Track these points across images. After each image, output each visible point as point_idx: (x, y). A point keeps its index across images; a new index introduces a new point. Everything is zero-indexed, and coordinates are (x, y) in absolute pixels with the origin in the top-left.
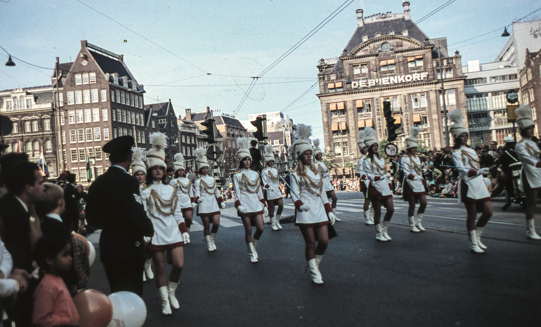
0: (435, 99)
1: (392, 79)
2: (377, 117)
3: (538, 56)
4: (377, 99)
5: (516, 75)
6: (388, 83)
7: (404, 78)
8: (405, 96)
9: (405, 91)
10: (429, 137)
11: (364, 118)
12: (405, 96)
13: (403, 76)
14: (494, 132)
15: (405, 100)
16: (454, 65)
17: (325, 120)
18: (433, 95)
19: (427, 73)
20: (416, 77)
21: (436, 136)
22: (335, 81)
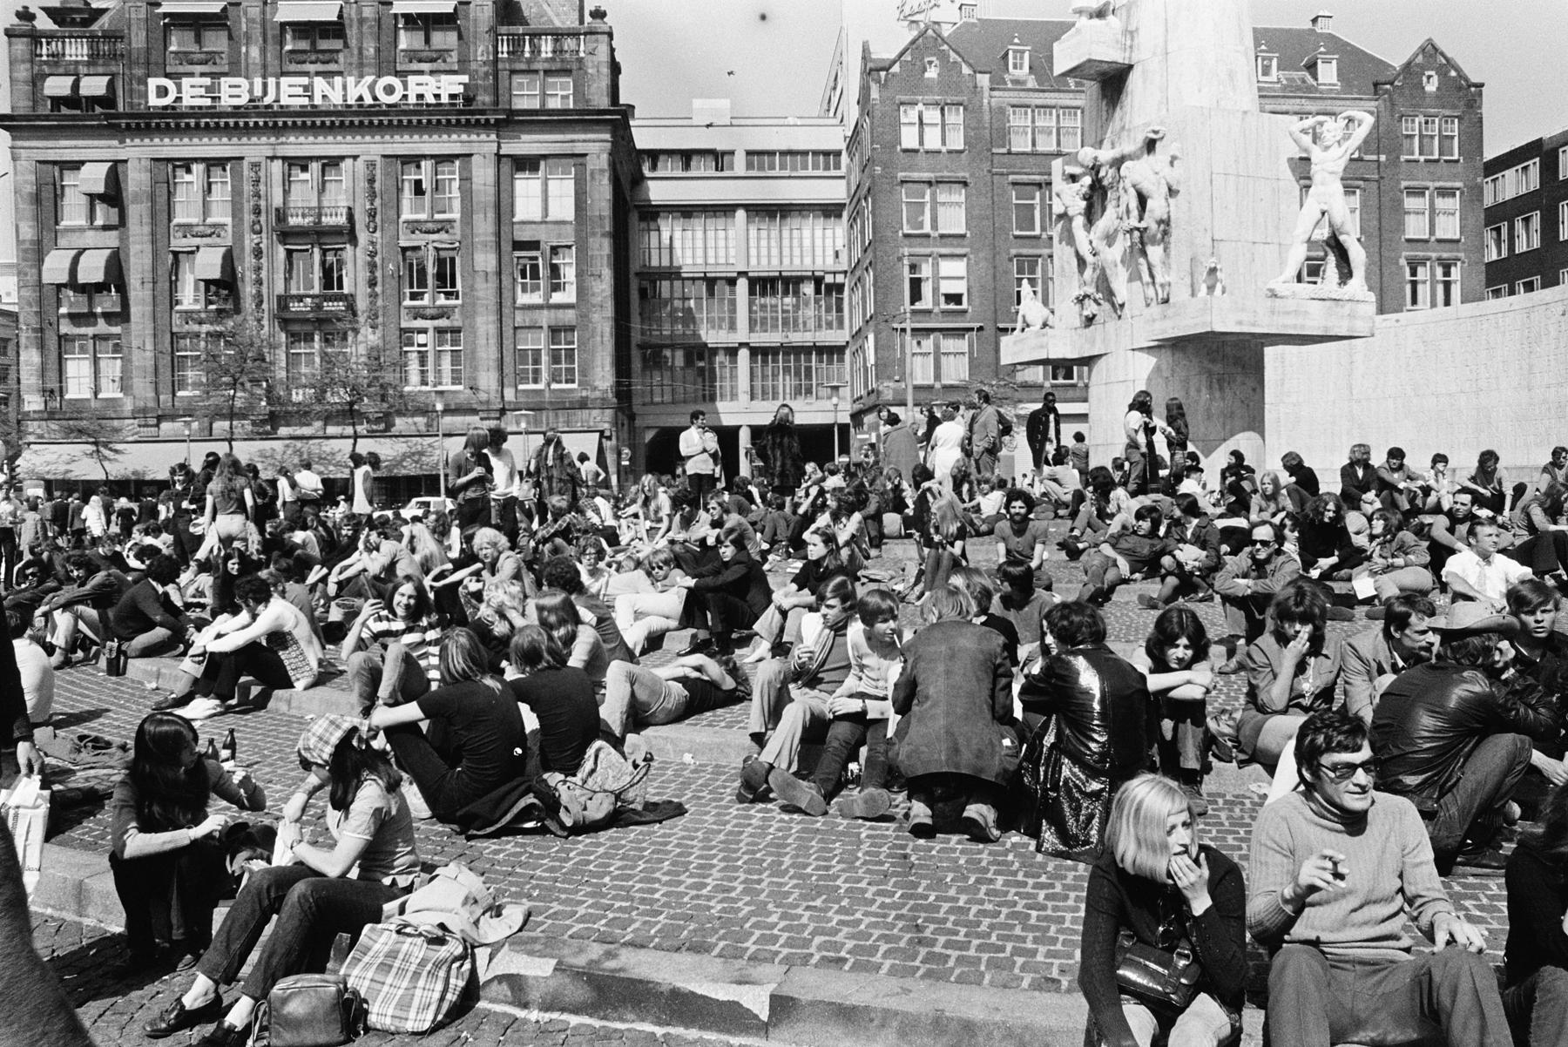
0: (492, 190)
1: (319, 83)
2: (249, 241)
3: (896, 69)
4: (255, 166)
5: (838, 154)
6: (306, 101)
7: (372, 88)
8: (371, 165)
9: (373, 147)
10: (455, 342)
11: (197, 241)
12: (371, 165)
13: (369, 79)
14: (744, 354)
15: (372, 181)
16: (580, 60)
17: (28, 232)
18: (483, 174)
19: (465, 79)
20: (420, 90)
21: (482, 341)
22: (82, 70)
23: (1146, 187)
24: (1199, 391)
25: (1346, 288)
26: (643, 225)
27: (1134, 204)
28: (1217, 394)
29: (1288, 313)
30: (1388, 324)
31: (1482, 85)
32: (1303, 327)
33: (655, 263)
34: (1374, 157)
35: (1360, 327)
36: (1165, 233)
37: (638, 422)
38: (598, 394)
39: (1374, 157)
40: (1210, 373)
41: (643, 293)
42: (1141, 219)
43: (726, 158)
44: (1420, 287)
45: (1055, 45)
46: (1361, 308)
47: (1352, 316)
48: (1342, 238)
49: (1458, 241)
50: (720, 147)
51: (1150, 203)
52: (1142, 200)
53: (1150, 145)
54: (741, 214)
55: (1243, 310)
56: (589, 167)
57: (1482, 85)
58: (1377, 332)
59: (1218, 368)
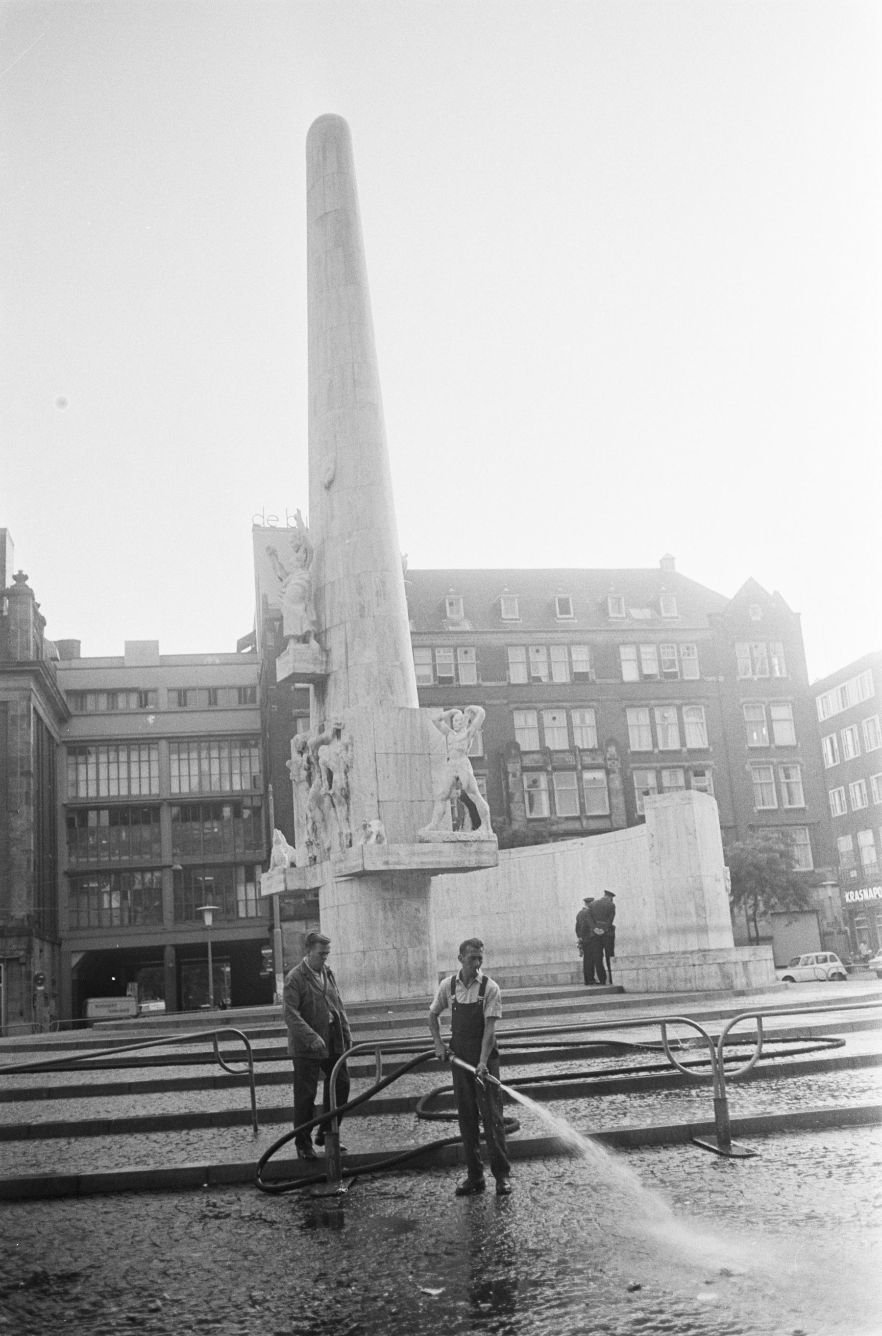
23: (332, 765)
24: (377, 912)
25: (477, 831)
26: (71, 760)
27: (325, 777)
28: (390, 914)
29: (425, 854)
30: (576, 846)
31: (799, 614)
32: (439, 863)
33: (82, 794)
34: (714, 678)
35: (485, 859)
36: (347, 797)
37: (65, 947)
38: (13, 924)
39: (714, 678)
40: (384, 899)
41: (70, 823)
42: (330, 787)
43: (150, 695)
44: (793, 786)
45: (277, 660)
46: (486, 847)
47: (478, 852)
48: (470, 796)
49: (795, 747)
50: (142, 685)
51: (335, 777)
52: (330, 775)
53: (338, 733)
54: (163, 744)
55: (389, 854)
56: (11, 713)
57: (799, 614)
58: (500, 862)
59: (388, 895)
